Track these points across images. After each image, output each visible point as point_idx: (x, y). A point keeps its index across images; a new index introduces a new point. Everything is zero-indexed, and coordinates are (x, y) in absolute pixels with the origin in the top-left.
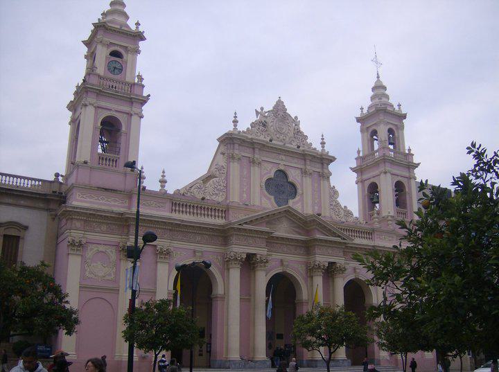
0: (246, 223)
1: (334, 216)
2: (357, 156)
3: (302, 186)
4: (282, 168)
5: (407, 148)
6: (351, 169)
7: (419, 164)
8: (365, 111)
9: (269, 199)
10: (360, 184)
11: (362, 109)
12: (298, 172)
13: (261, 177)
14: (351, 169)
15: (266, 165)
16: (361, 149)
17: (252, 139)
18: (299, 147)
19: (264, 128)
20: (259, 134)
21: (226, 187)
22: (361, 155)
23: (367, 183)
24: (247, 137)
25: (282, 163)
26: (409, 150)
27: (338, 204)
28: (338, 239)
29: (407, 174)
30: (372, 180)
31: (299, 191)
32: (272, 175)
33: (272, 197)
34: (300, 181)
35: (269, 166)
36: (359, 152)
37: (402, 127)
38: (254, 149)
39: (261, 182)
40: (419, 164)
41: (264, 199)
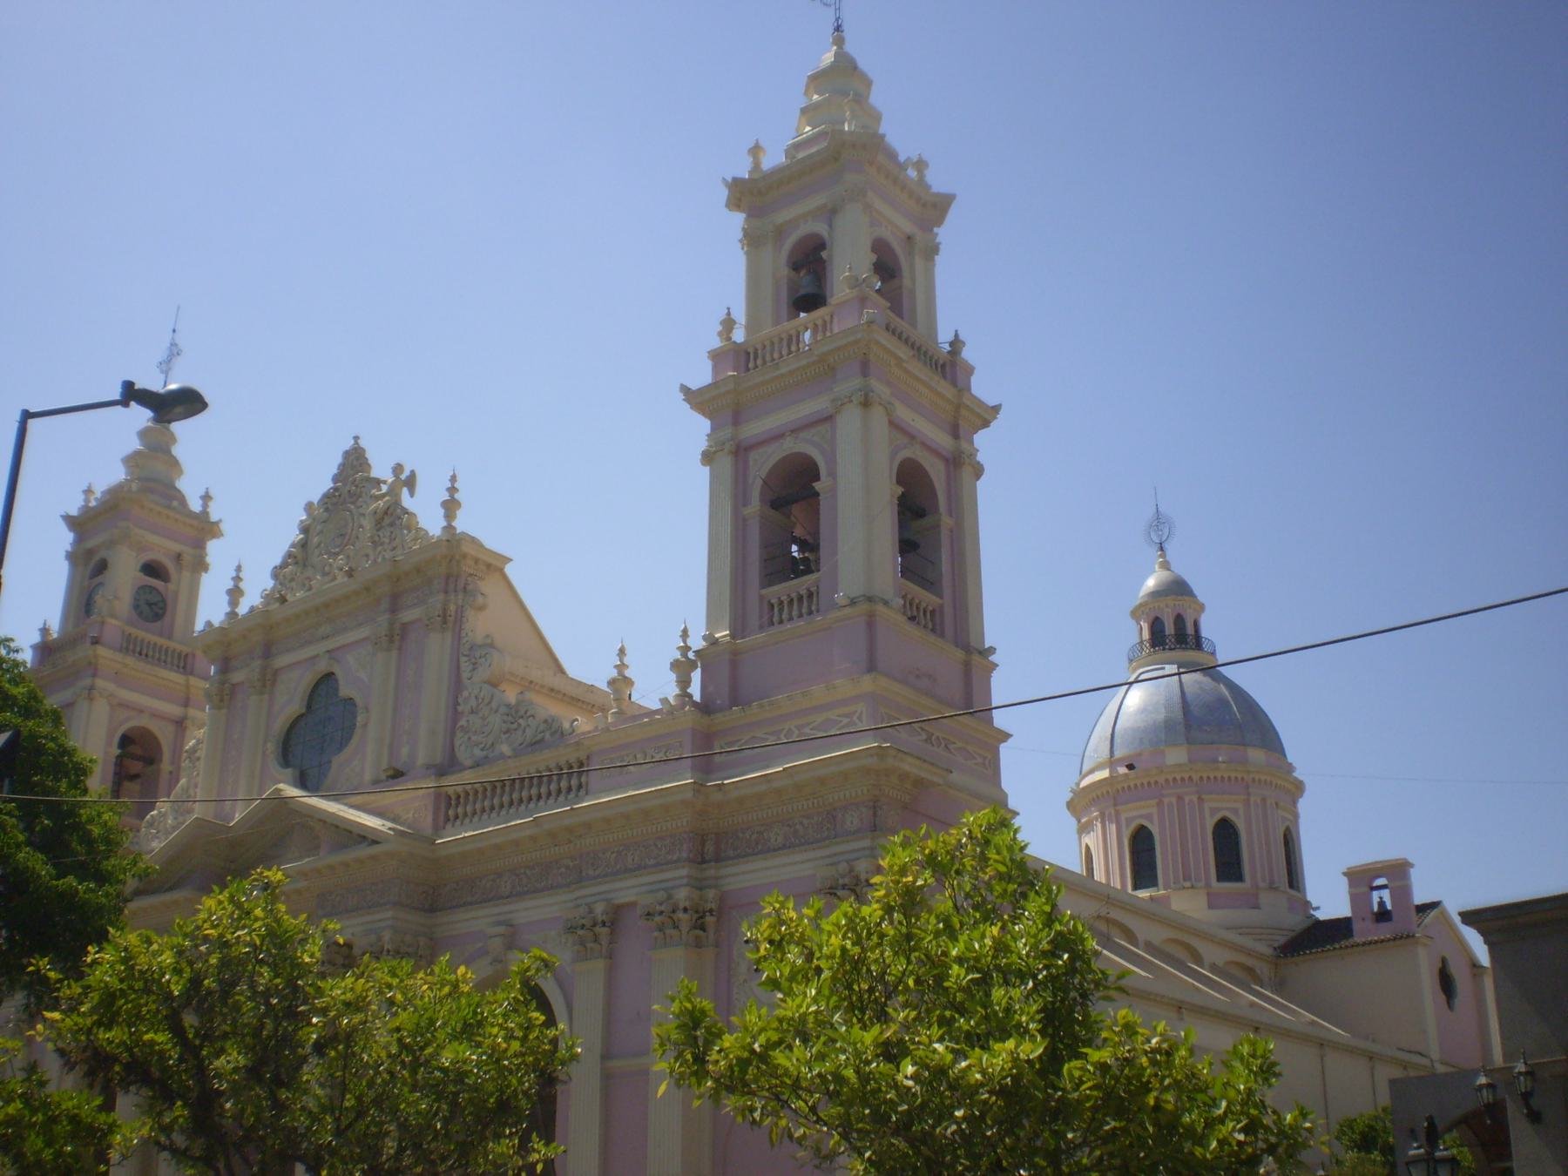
2: (716, 343)
5: (944, 337)
6: (687, 393)
7: (996, 409)
8: (774, 158)
10: (726, 463)
11: (756, 150)
14: (687, 393)
16: (740, 315)
22: (739, 336)
23: (763, 462)
26: (956, 344)
29: (943, 440)
30: (790, 446)
36: (728, 324)
37: (932, 250)
40: (996, 409)
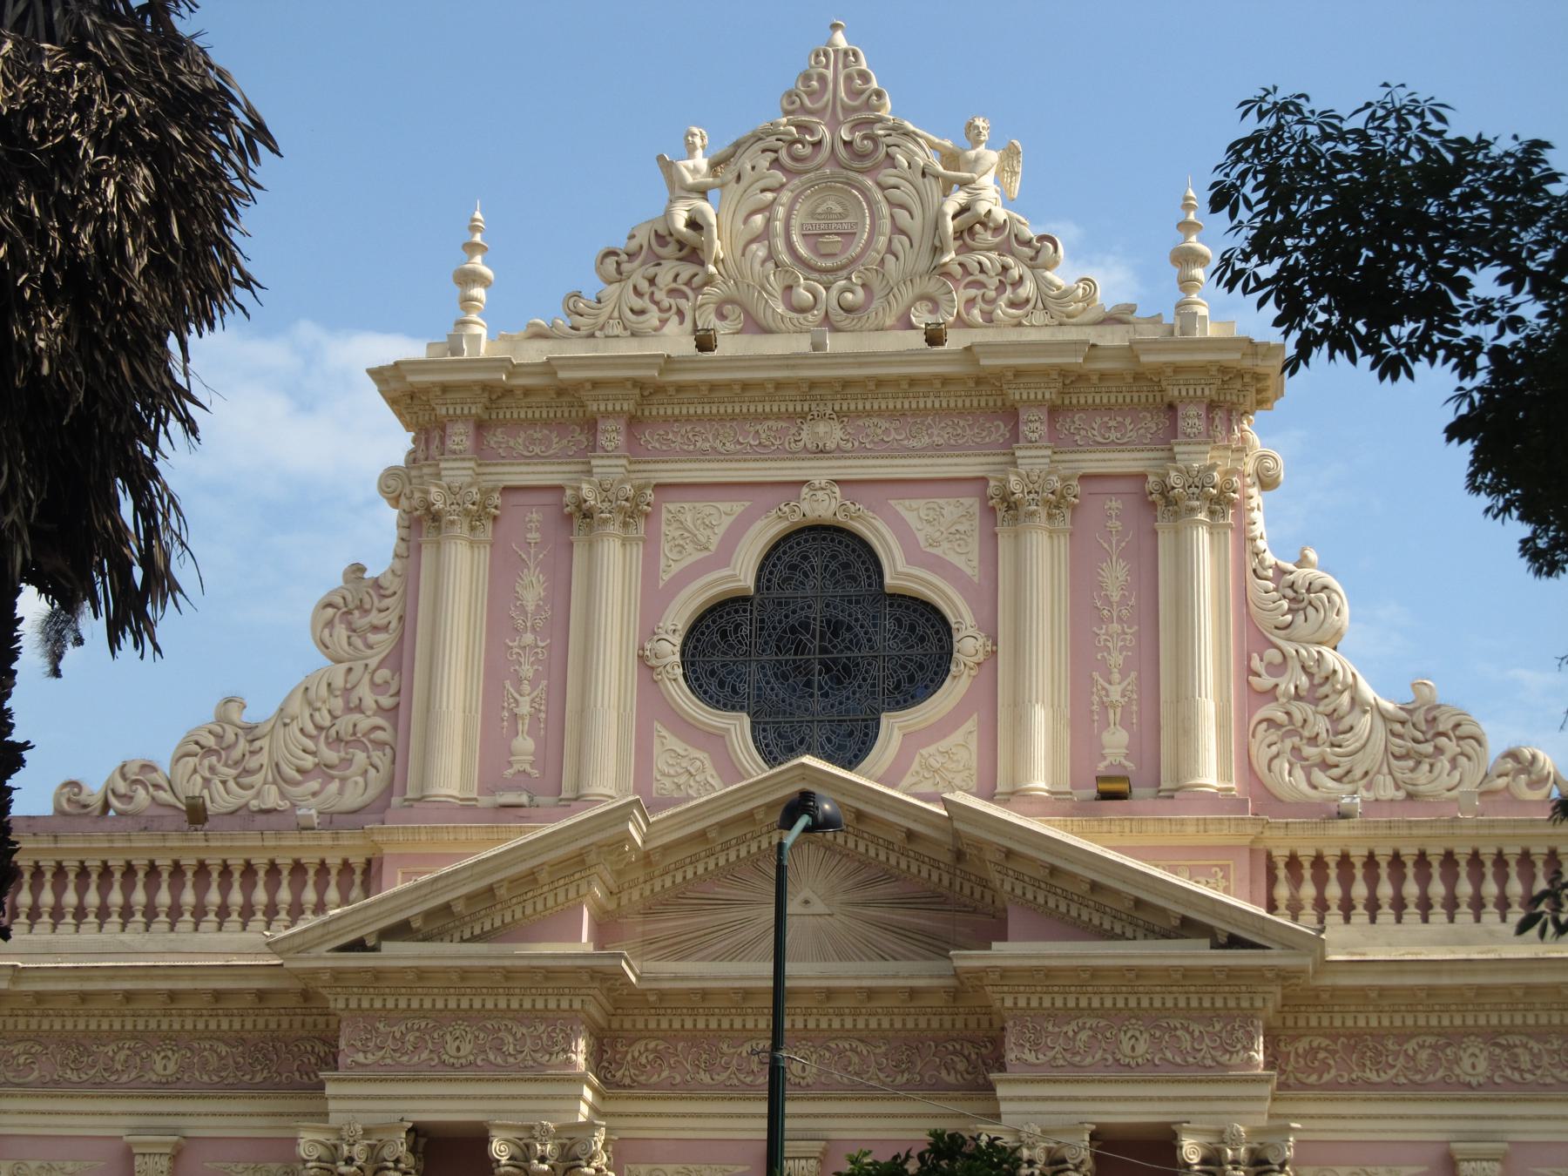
0: (401, 931)
1: (1290, 780)
3: (987, 597)
4: (822, 507)
9: (714, 741)
12: (959, 511)
13: (653, 598)
15: (689, 511)
17: (549, 367)
18: (934, 337)
19: (687, 270)
20: (653, 317)
21: (392, 712)
24: (514, 369)
25: (819, 472)
27: (1321, 683)
28: (1195, 954)
31: (968, 645)
32: (742, 574)
33: (737, 727)
34: (967, 558)
35: (725, 511)
38: (591, 425)
39: (650, 631)
41: (668, 745)
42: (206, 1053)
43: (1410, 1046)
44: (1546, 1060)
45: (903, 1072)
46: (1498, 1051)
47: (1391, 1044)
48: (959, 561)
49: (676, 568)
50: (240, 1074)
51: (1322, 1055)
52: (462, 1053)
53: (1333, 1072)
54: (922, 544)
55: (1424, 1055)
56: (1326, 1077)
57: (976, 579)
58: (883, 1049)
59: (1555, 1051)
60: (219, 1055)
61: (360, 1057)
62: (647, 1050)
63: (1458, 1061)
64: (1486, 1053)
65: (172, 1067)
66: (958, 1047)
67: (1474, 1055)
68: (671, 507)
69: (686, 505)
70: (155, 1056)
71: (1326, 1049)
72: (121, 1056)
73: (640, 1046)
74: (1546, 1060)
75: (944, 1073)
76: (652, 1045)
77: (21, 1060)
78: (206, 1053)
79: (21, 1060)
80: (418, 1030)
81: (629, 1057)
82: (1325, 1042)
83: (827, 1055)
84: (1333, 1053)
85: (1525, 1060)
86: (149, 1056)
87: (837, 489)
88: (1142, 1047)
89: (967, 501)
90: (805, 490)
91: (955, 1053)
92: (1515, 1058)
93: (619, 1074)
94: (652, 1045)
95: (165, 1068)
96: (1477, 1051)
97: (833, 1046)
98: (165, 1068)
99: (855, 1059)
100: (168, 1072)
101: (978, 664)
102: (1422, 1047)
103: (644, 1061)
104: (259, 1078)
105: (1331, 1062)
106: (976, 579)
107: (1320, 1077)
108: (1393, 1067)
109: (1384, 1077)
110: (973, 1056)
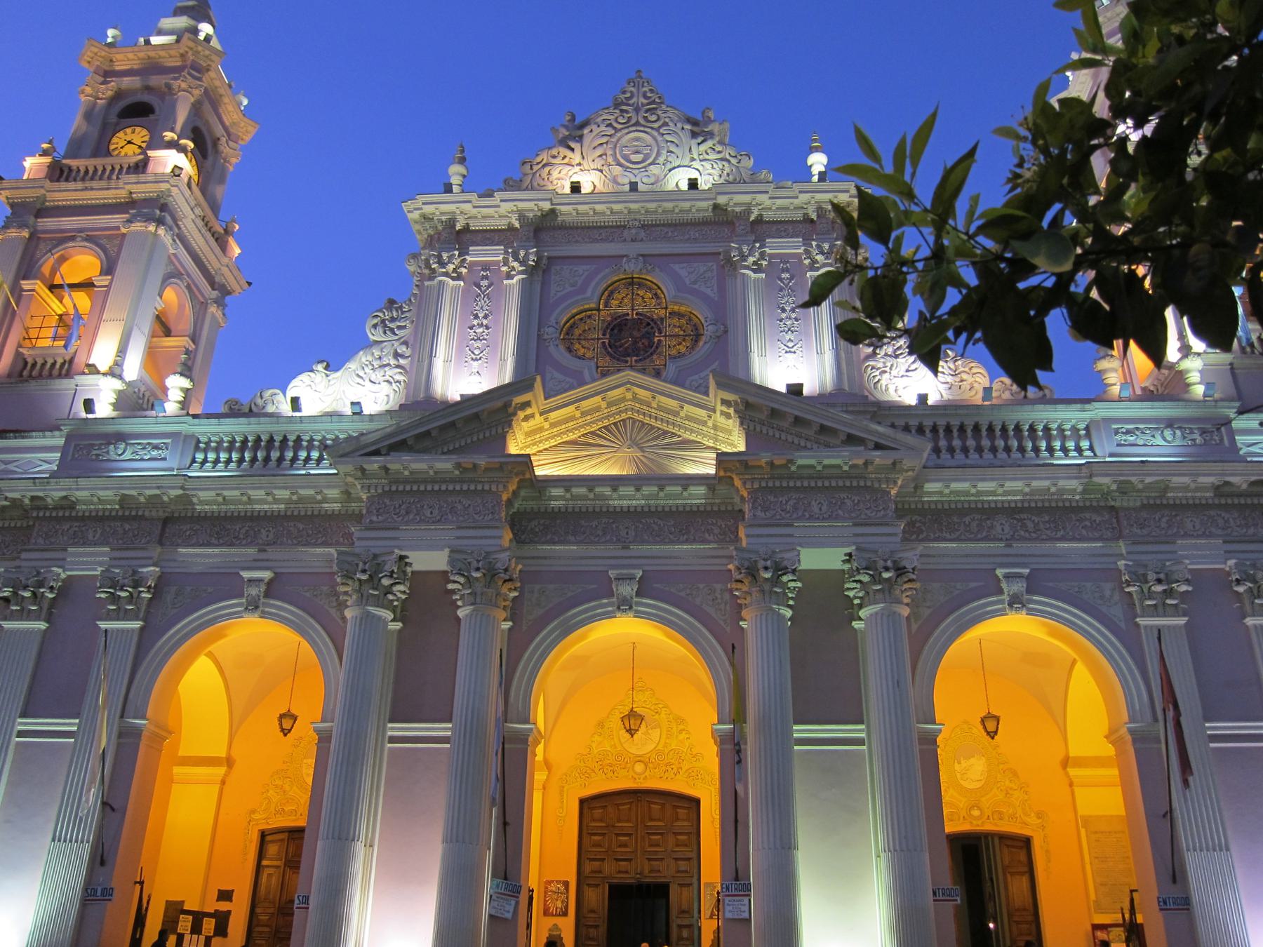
42: (291, 528)
43: (967, 519)
44: (1042, 526)
45: (683, 535)
46: (1015, 522)
47: (955, 519)
48: (708, 291)
49: (559, 294)
50: (309, 539)
51: (917, 525)
52: (434, 515)
53: (925, 534)
54: (688, 283)
55: (974, 524)
56: (921, 537)
57: (716, 299)
58: (672, 523)
59: (1047, 522)
60: (298, 529)
61: (375, 518)
62: (539, 524)
63: (992, 527)
64: (1008, 523)
65: (271, 536)
66: (714, 522)
67: (1001, 524)
68: (558, 268)
69: (565, 267)
70: (262, 530)
71: (920, 521)
72: (243, 531)
73: (535, 523)
74: (1042, 526)
75: (707, 535)
76: (542, 522)
77: (188, 533)
78: (291, 528)
79: (188, 533)
80: (409, 503)
81: (529, 528)
82: (919, 518)
83: (641, 526)
84: (924, 524)
85: (1030, 525)
86: (259, 530)
87: (640, 258)
88: (824, 508)
89: (710, 264)
90: (625, 259)
91: (713, 524)
92: (1024, 526)
93: (523, 537)
94: (542, 522)
95: (268, 536)
96: (1004, 522)
97: (644, 521)
98: (268, 536)
99: (657, 528)
100: (269, 538)
101: (718, 337)
102: (973, 520)
103: (537, 530)
104: (320, 541)
105: (924, 528)
106: (716, 299)
107: (918, 536)
108: (958, 530)
109: (954, 536)
110: (723, 526)
